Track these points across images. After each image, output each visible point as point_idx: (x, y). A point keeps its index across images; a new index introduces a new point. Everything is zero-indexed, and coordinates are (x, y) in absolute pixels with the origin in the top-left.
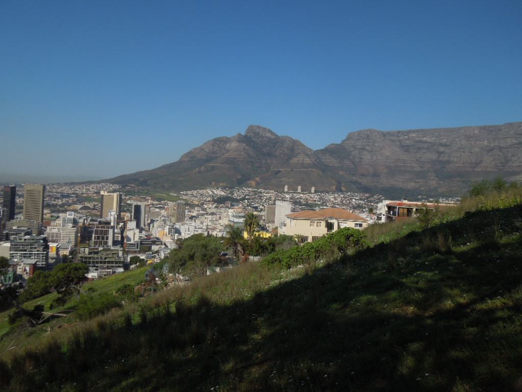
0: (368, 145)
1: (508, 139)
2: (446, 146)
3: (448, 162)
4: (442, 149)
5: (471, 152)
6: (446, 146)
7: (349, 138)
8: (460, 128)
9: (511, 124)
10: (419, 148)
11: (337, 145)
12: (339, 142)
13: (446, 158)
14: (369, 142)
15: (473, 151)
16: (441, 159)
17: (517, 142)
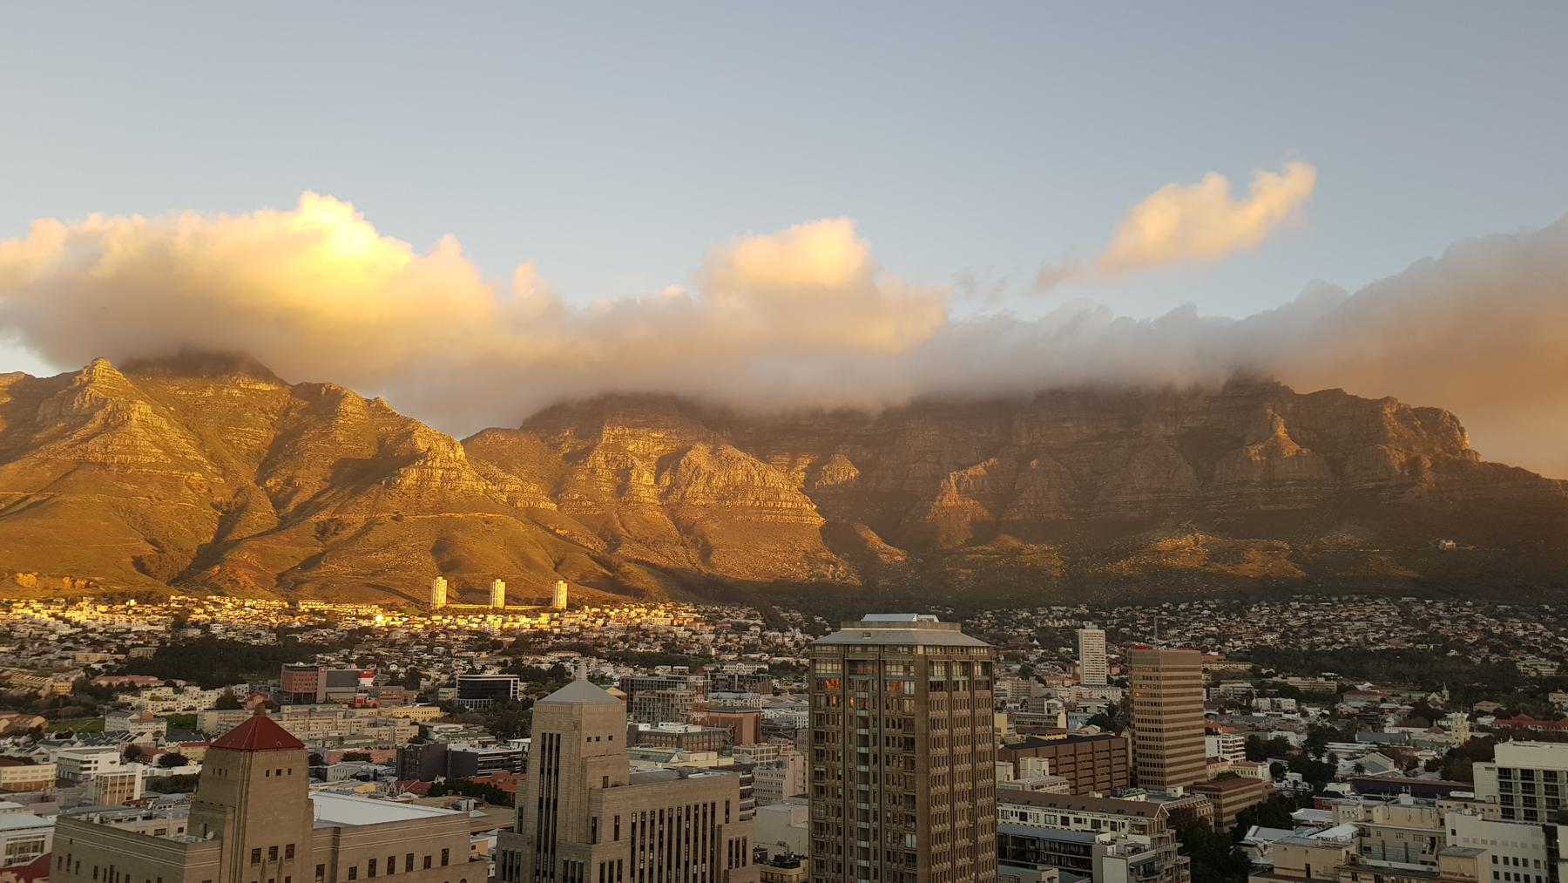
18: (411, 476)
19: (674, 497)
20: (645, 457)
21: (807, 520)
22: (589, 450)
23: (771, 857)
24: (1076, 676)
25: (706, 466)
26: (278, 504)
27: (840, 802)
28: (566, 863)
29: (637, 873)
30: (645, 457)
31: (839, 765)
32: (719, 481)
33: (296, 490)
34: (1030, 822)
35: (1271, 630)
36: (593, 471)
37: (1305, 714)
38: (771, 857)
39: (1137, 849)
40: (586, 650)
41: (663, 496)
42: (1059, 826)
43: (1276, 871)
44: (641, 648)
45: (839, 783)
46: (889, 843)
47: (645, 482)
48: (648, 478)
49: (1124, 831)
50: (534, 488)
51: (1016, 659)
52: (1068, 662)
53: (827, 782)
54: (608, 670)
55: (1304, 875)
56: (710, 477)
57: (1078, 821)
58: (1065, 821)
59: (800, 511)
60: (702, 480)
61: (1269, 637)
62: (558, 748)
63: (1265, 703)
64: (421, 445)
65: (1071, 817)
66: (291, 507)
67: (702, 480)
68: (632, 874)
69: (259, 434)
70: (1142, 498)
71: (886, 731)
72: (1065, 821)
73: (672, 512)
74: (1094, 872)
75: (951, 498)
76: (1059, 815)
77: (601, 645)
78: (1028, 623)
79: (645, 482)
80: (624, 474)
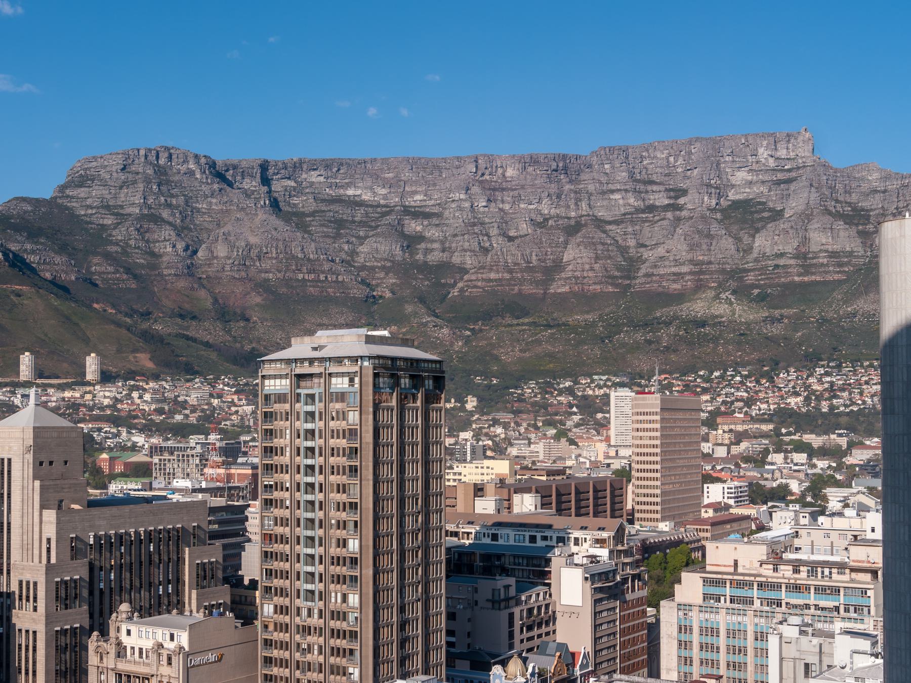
0: (169, 205)
1: (617, 196)
2: (427, 216)
3: (445, 267)
4: (414, 226)
5: (511, 239)
6: (427, 216)
7: (81, 180)
10: (340, 224)
11: (37, 203)
12: (46, 192)
13: (435, 257)
14: (172, 196)
15: (512, 233)
16: (420, 257)
17: (640, 204)
23: (246, 582)
24: (608, 439)
27: (286, 513)
28: (21, 582)
29: (97, 593)
31: (287, 477)
34: (501, 542)
35: (797, 394)
37: (814, 466)
38: (246, 582)
39: (593, 559)
40: (116, 421)
42: (527, 544)
43: (708, 568)
44: (178, 418)
45: (287, 495)
46: (334, 551)
49: (586, 545)
51: (549, 423)
52: (603, 426)
53: (277, 495)
54: (139, 439)
55: (732, 570)
57: (545, 538)
58: (533, 539)
61: (793, 401)
62: (9, 472)
63: (778, 458)
65: (539, 535)
68: (91, 593)
70: (685, 269)
71: (333, 442)
72: (533, 539)
74: (553, 581)
76: (527, 534)
77: (136, 417)
78: (570, 391)
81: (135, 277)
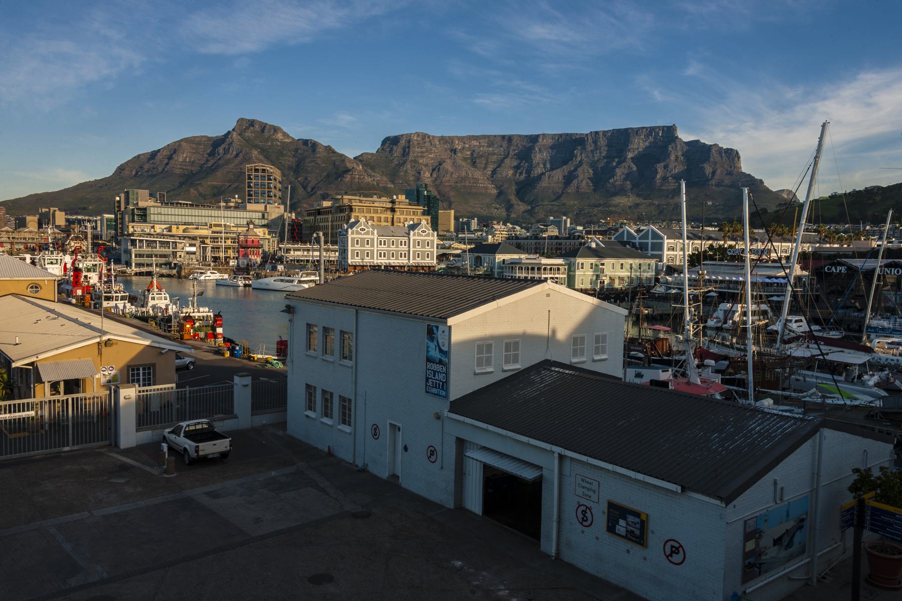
8: (538, 136)
9: (597, 133)
18: (348, 178)
19: (438, 182)
20: (426, 165)
21: (489, 191)
22: (404, 163)
25: (450, 169)
26: (305, 188)
30: (426, 165)
32: (455, 176)
33: (309, 182)
36: (406, 171)
41: (434, 182)
47: (426, 175)
48: (427, 174)
50: (385, 178)
56: (452, 173)
59: (486, 188)
60: (449, 175)
64: (349, 165)
66: (309, 189)
67: (449, 175)
69: (290, 161)
73: (437, 187)
75: (544, 183)
79: (426, 175)
80: (419, 173)
81: (409, 185)
